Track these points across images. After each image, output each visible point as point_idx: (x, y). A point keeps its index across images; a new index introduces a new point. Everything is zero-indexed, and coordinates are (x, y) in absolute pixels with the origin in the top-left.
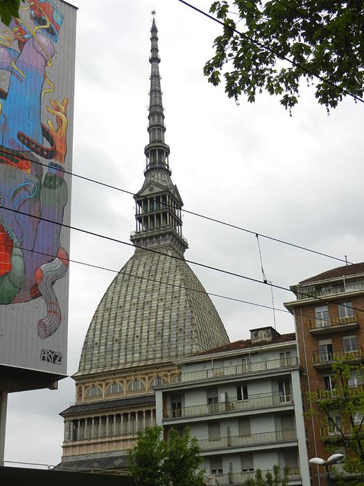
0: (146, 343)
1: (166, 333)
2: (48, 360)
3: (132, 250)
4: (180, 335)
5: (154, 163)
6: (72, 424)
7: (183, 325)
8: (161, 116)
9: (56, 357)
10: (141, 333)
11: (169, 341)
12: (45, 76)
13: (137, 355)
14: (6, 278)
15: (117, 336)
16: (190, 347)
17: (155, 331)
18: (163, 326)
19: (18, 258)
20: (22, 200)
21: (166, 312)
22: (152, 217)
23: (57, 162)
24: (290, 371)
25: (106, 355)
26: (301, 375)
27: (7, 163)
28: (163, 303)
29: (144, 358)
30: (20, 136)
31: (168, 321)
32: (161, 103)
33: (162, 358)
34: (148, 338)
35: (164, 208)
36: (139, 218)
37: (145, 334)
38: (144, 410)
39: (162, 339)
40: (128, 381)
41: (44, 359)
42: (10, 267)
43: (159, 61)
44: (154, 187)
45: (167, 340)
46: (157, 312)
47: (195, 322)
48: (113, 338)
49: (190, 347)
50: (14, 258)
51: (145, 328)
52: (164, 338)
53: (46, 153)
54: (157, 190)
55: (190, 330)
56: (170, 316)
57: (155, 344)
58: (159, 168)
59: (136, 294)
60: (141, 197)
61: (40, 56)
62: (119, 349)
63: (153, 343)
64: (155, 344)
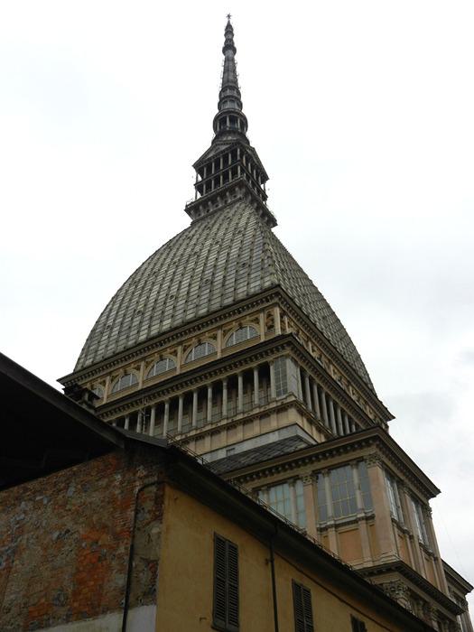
3: (186, 221)
15: (140, 307)
36: (198, 187)
43: (234, 51)
48: (135, 311)
49: (258, 283)
51: (185, 283)
54: (223, 148)
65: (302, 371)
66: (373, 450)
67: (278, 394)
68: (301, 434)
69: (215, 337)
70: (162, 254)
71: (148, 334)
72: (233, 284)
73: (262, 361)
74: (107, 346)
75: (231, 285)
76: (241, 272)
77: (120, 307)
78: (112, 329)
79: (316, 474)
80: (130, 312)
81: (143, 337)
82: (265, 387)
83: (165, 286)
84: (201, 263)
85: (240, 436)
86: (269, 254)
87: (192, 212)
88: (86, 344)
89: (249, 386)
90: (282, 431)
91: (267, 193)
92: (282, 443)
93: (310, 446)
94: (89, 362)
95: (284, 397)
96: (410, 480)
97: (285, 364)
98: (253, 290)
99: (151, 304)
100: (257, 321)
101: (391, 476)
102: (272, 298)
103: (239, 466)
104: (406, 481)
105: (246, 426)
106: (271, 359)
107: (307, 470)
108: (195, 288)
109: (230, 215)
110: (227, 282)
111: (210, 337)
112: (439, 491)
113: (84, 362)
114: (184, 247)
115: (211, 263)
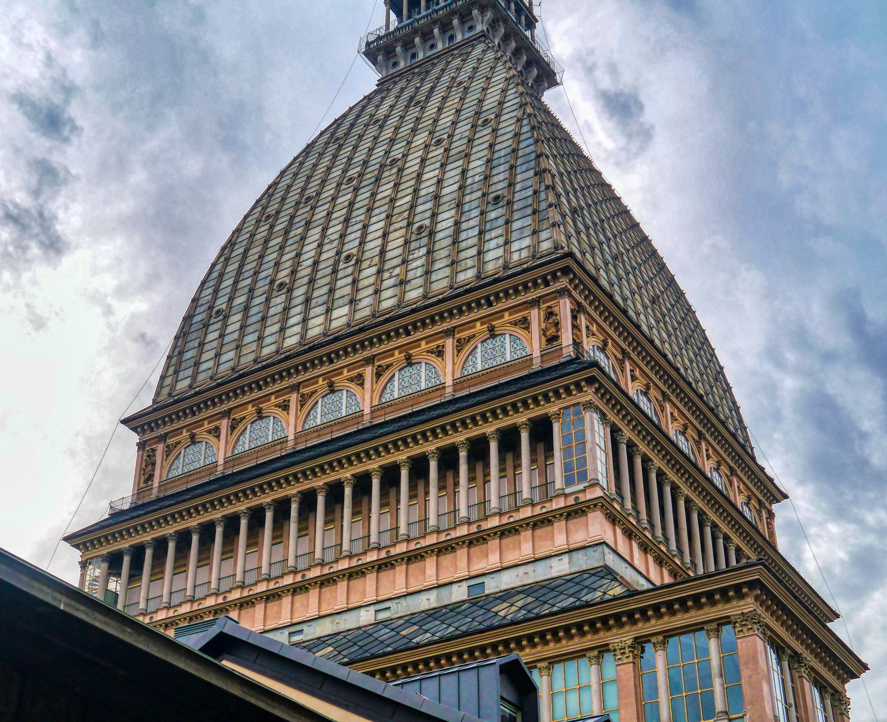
10: (363, 242)
15: (283, 275)
18: (437, 205)
25: (242, 336)
34: (383, 252)
37: (373, 245)
45: (449, 241)
48: (272, 282)
49: (527, 242)
51: (376, 227)
55: (530, 192)
56: (464, 172)
59: (359, 157)
62: (287, 309)
65: (615, 431)
66: (748, 605)
67: (569, 481)
68: (611, 560)
69: (440, 353)
70: (321, 155)
71: (303, 335)
72: (475, 240)
73: (536, 412)
74: (218, 355)
75: (470, 242)
76: (493, 215)
77: (239, 271)
78: (227, 317)
79: (640, 643)
80: (262, 286)
81: (291, 341)
82: (541, 458)
83: (334, 231)
84: (407, 186)
85: (493, 560)
86: (549, 181)
87: (380, 58)
88: (175, 347)
89: (509, 457)
90: (575, 555)
91: (536, 11)
92: (576, 580)
93: (633, 593)
94: (183, 385)
95: (580, 487)
96: (812, 651)
97: (582, 420)
98: (515, 257)
99: (304, 271)
100: (525, 323)
101: (779, 647)
102: (555, 278)
103: (496, 622)
104: (806, 654)
105: (505, 541)
106: (555, 409)
107: (622, 637)
109: (463, 76)
110: (463, 236)
111: (431, 352)
112: (865, 667)
113: (173, 386)
114: (366, 144)
115: (428, 188)
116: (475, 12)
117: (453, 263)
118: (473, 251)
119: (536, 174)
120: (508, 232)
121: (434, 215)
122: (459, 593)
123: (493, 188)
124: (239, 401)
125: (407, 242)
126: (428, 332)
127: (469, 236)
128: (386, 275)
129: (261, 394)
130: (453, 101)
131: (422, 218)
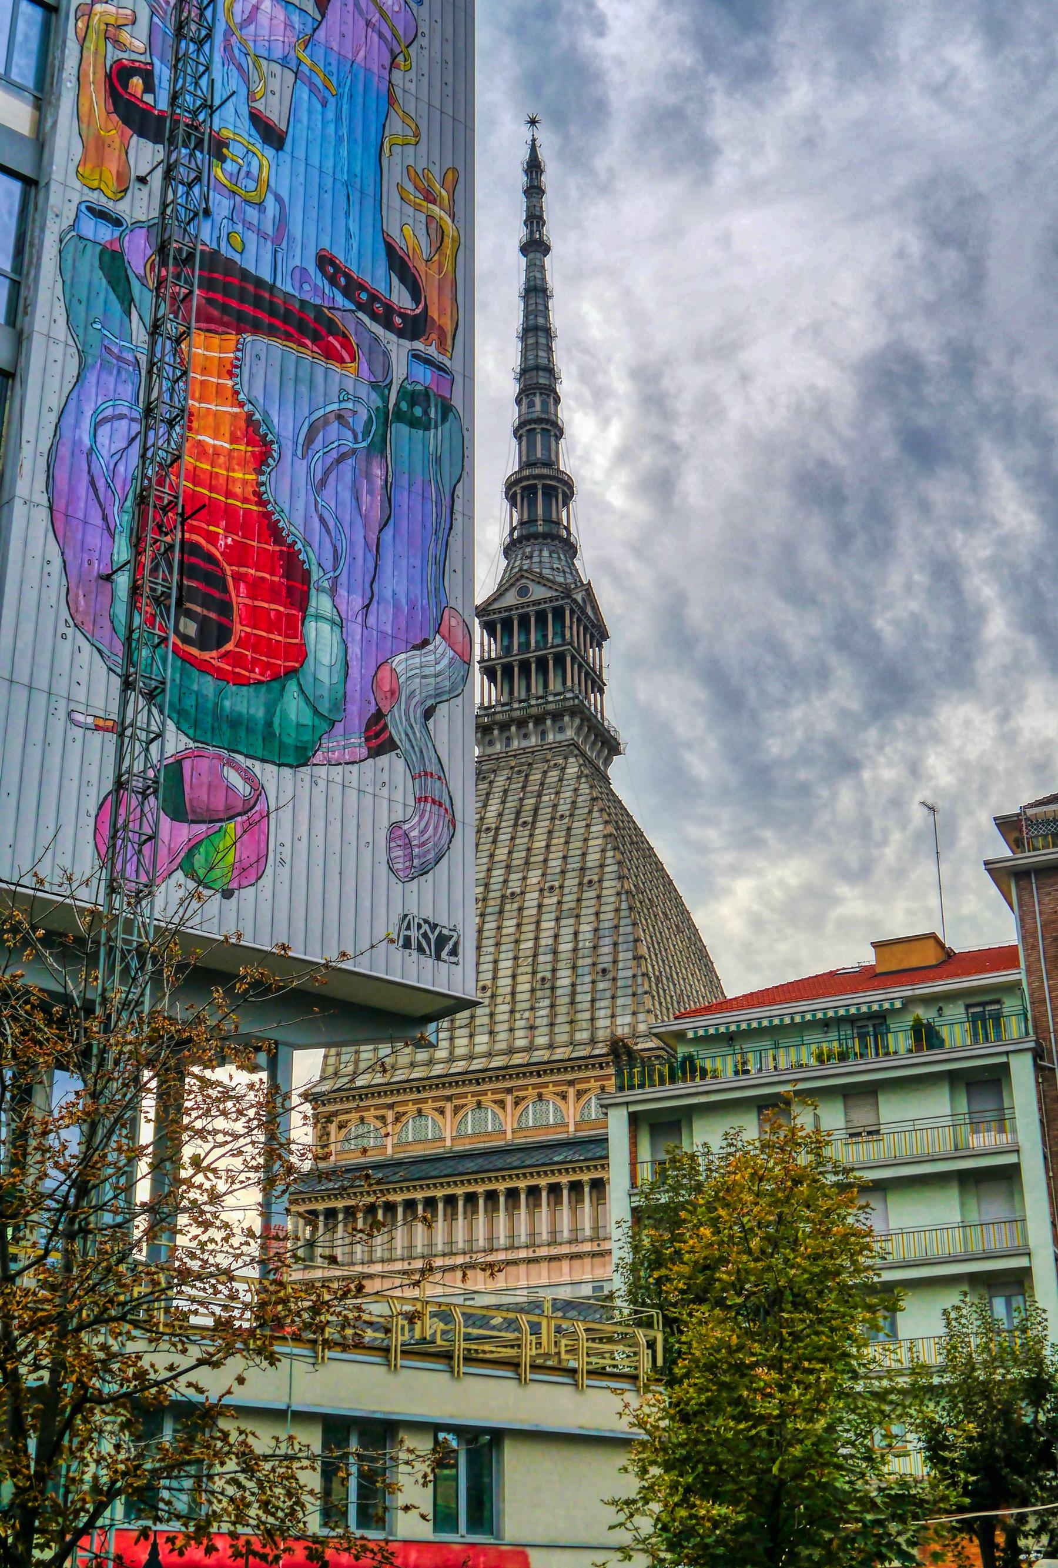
0: (507, 1008)
1: (564, 980)
2: (421, 949)
4: (601, 986)
5: (532, 521)
6: (301, 1222)
7: (609, 958)
8: (550, 394)
9: (442, 941)
10: (495, 978)
11: (573, 1003)
12: (391, 100)
13: (482, 1039)
14: (292, 686)
16: (628, 1019)
17: (534, 973)
18: (556, 961)
19: (325, 627)
20: (334, 454)
21: (563, 922)
22: (525, 666)
23: (432, 351)
24: (1007, 1053)
26: (1038, 1069)
27: (288, 337)
28: (554, 900)
29: (503, 1046)
30: (325, 261)
31: (570, 946)
32: (550, 359)
33: (551, 1046)
34: (513, 994)
35: (558, 641)
37: (505, 982)
38: (501, 1187)
39: (553, 996)
40: (457, 1109)
41: (407, 944)
42: (300, 653)
43: (546, 249)
44: (532, 586)
45: (567, 1000)
46: (538, 923)
47: (643, 950)
49: (628, 1019)
50: (311, 628)
51: (506, 965)
52: (559, 992)
53: (398, 320)
54: (539, 592)
55: (629, 973)
56: (576, 934)
57: (532, 1009)
58: (545, 536)
60: (494, 612)
61: (376, 37)
63: (527, 1005)
64: (532, 1009)
108: (524, 987)
115: (546, 941)
116: (567, 718)
117: (571, 1022)
118: (587, 1015)
119: (634, 958)
120: (614, 1006)
121: (554, 970)
122: (587, 1290)
123: (602, 959)
124: (400, 1098)
125: (533, 990)
126: (554, 1078)
127: (584, 999)
128: (518, 1016)
129: (420, 1096)
130: (558, 840)
131: (544, 971)
